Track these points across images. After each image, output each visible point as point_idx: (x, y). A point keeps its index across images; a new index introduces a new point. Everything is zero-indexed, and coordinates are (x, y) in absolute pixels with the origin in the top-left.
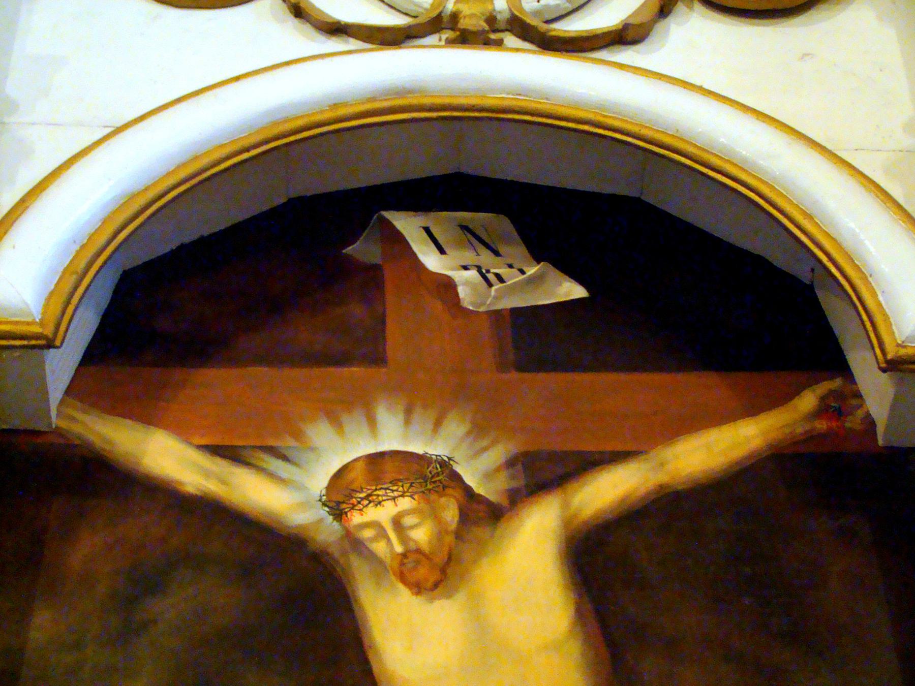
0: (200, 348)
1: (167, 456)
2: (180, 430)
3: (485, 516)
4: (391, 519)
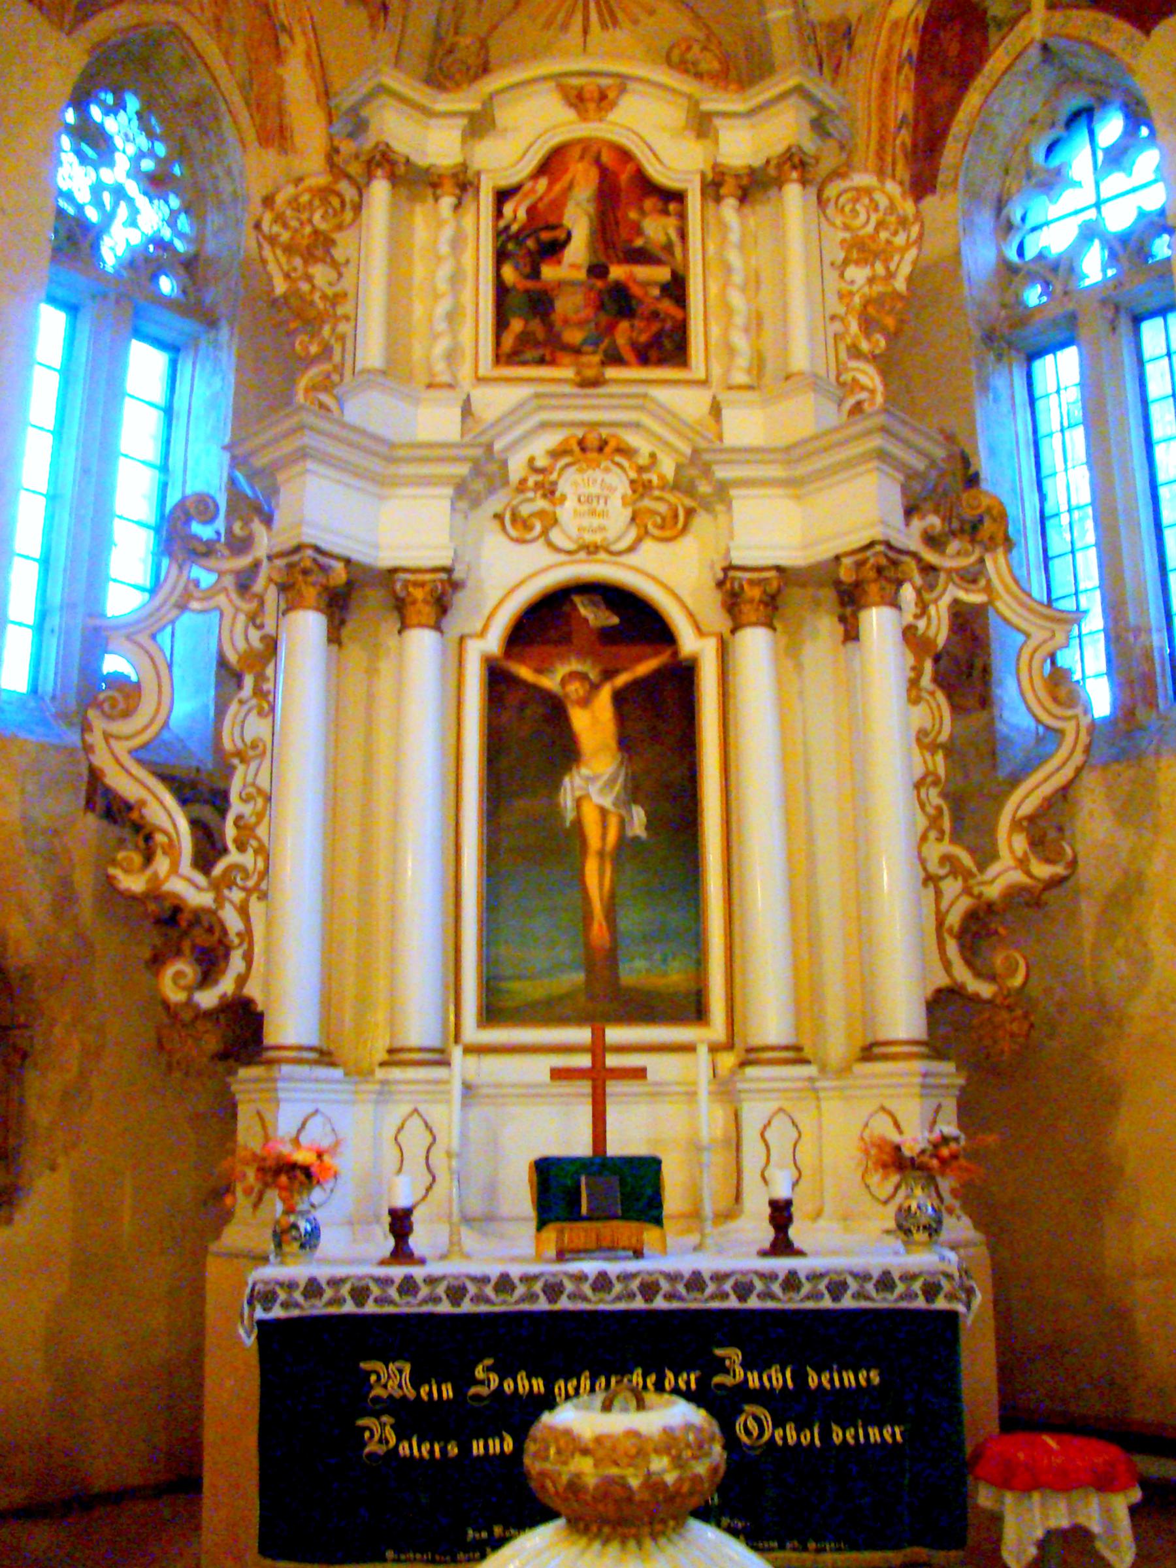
0: (530, 643)
1: (525, 672)
2: (529, 667)
3: (595, 687)
4: (575, 689)
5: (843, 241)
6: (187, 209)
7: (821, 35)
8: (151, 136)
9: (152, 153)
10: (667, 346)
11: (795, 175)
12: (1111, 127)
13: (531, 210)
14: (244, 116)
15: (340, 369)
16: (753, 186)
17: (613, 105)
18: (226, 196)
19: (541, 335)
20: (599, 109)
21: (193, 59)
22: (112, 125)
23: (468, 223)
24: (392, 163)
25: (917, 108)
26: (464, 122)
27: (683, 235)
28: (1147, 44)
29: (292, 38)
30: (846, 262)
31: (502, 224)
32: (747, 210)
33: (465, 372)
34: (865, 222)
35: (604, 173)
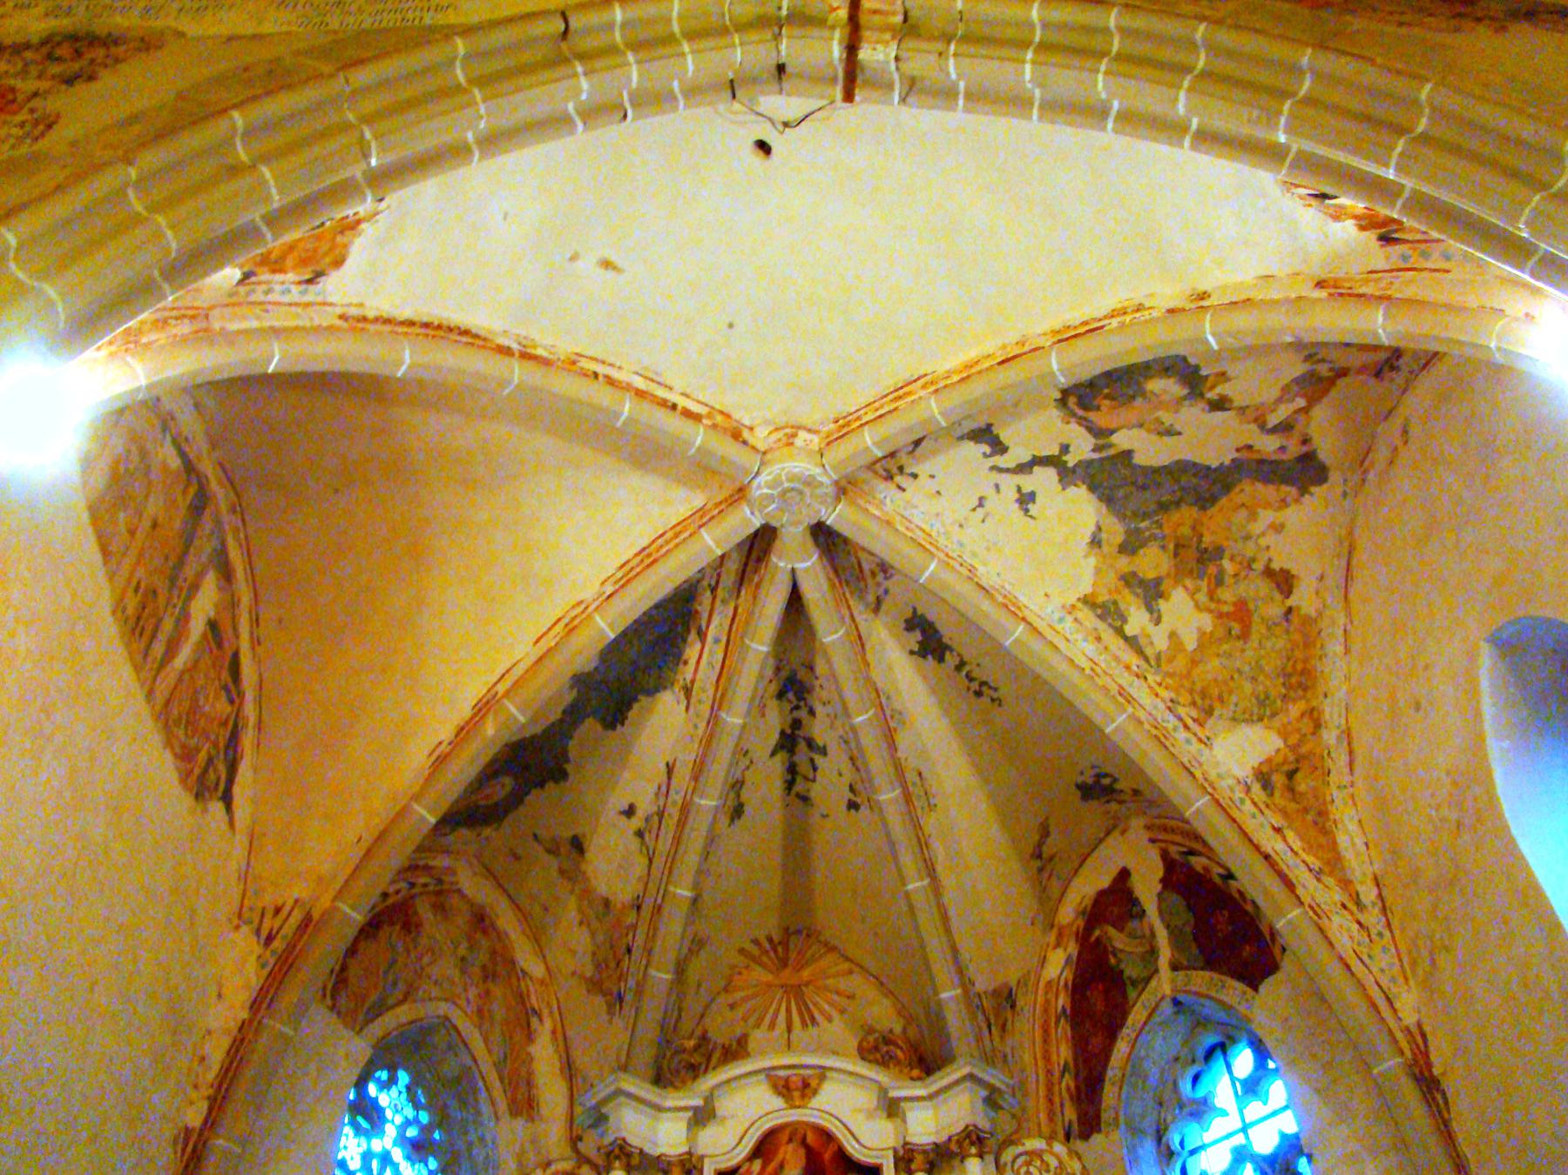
8: (417, 1106)
9: (416, 1121)
11: (973, 1150)
12: (1243, 1060)
14: (498, 1092)
17: (815, 1092)
20: (803, 1096)
22: (384, 1099)
24: (629, 1155)
25: (1075, 1054)
26: (690, 1114)
28: (1258, 1000)
29: (541, 1020)
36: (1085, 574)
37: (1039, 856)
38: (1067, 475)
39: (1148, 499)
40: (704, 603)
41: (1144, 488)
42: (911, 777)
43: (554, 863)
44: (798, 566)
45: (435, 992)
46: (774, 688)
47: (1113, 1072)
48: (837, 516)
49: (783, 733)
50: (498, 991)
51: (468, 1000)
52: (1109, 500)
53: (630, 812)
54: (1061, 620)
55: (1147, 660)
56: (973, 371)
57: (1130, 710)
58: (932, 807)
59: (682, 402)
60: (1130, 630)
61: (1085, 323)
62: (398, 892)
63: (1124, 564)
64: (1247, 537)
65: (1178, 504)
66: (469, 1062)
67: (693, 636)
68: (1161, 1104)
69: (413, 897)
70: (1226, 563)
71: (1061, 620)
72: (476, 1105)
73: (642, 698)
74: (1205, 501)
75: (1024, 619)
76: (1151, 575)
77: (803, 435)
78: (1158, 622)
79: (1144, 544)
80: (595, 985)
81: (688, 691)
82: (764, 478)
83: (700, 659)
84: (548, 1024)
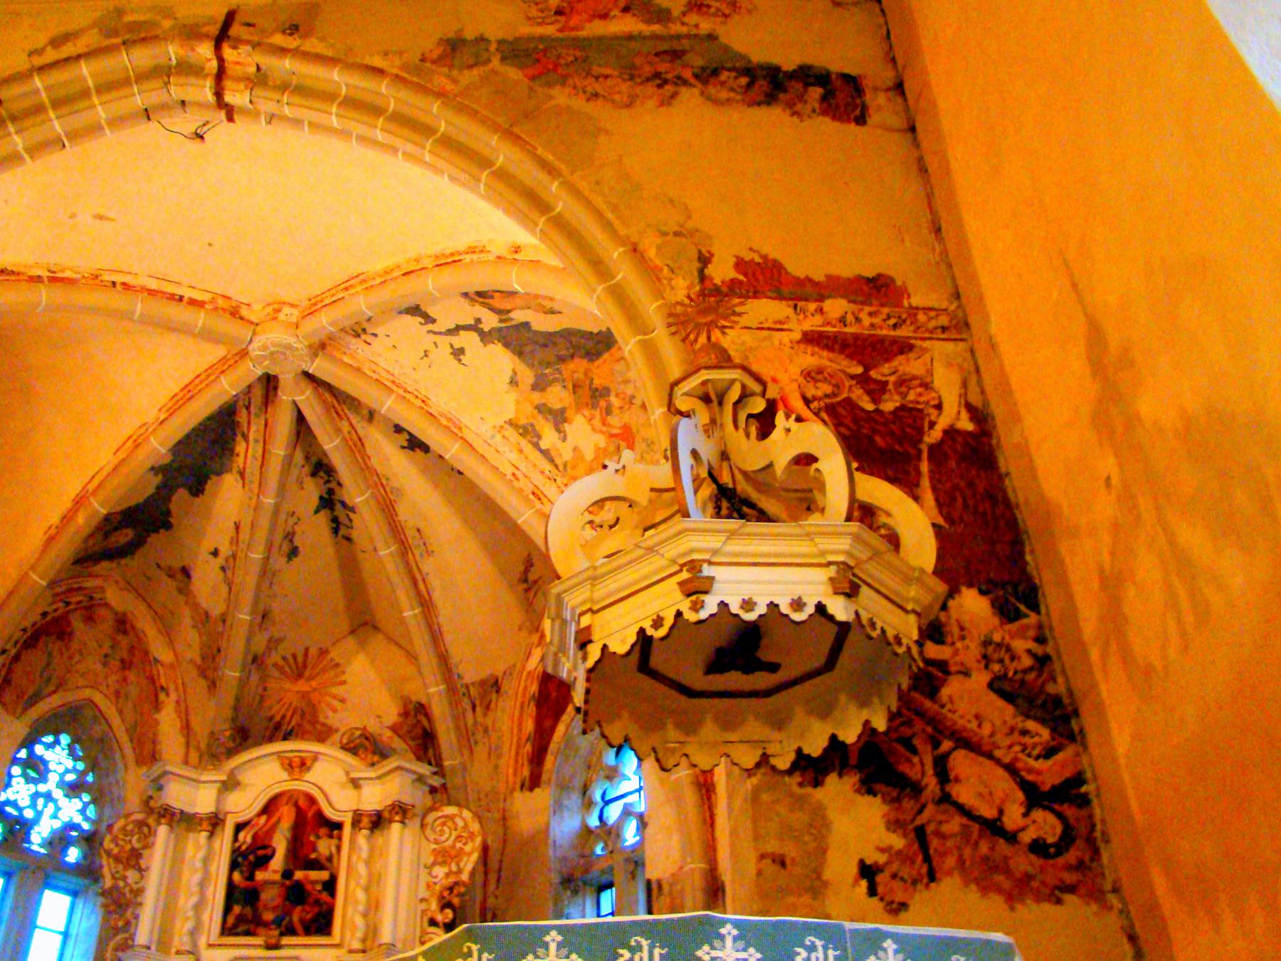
5: (434, 850)
6: (94, 801)
7: (472, 690)
8: (76, 758)
10: (321, 924)
11: (397, 818)
13: (255, 836)
14: (128, 750)
15: (132, 937)
16: (378, 821)
17: (309, 769)
18: (115, 795)
19: (250, 916)
21: (100, 715)
22: (48, 755)
23: (217, 843)
26: (218, 785)
27: (339, 848)
29: (168, 694)
30: (434, 864)
31: (237, 845)
32: (377, 832)
33: (202, 942)
34: (448, 837)
35: (300, 813)
36: (509, 405)
37: (526, 581)
38: (485, 337)
39: (550, 354)
40: (242, 417)
41: (546, 346)
42: (411, 533)
43: (171, 584)
44: (297, 399)
45: (82, 682)
46: (307, 469)
47: (553, 746)
48: (320, 367)
49: (321, 498)
50: (132, 676)
51: (108, 686)
52: (520, 354)
53: (215, 553)
54: (493, 437)
55: (556, 467)
56: (388, 277)
57: (538, 504)
58: (429, 553)
59: (188, 293)
60: (544, 445)
61: (452, 254)
62: (56, 610)
63: (537, 397)
64: (627, 382)
65: (572, 357)
66: (106, 728)
67: (239, 438)
68: (589, 767)
69: (69, 612)
70: (613, 399)
71: (493, 437)
72: (113, 759)
73: (214, 478)
74: (592, 355)
75: (462, 438)
76: (557, 406)
77: (286, 310)
78: (564, 439)
79: (549, 384)
80: (203, 673)
81: (242, 475)
82: (255, 345)
83: (246, 452)
84: (173, 696)
